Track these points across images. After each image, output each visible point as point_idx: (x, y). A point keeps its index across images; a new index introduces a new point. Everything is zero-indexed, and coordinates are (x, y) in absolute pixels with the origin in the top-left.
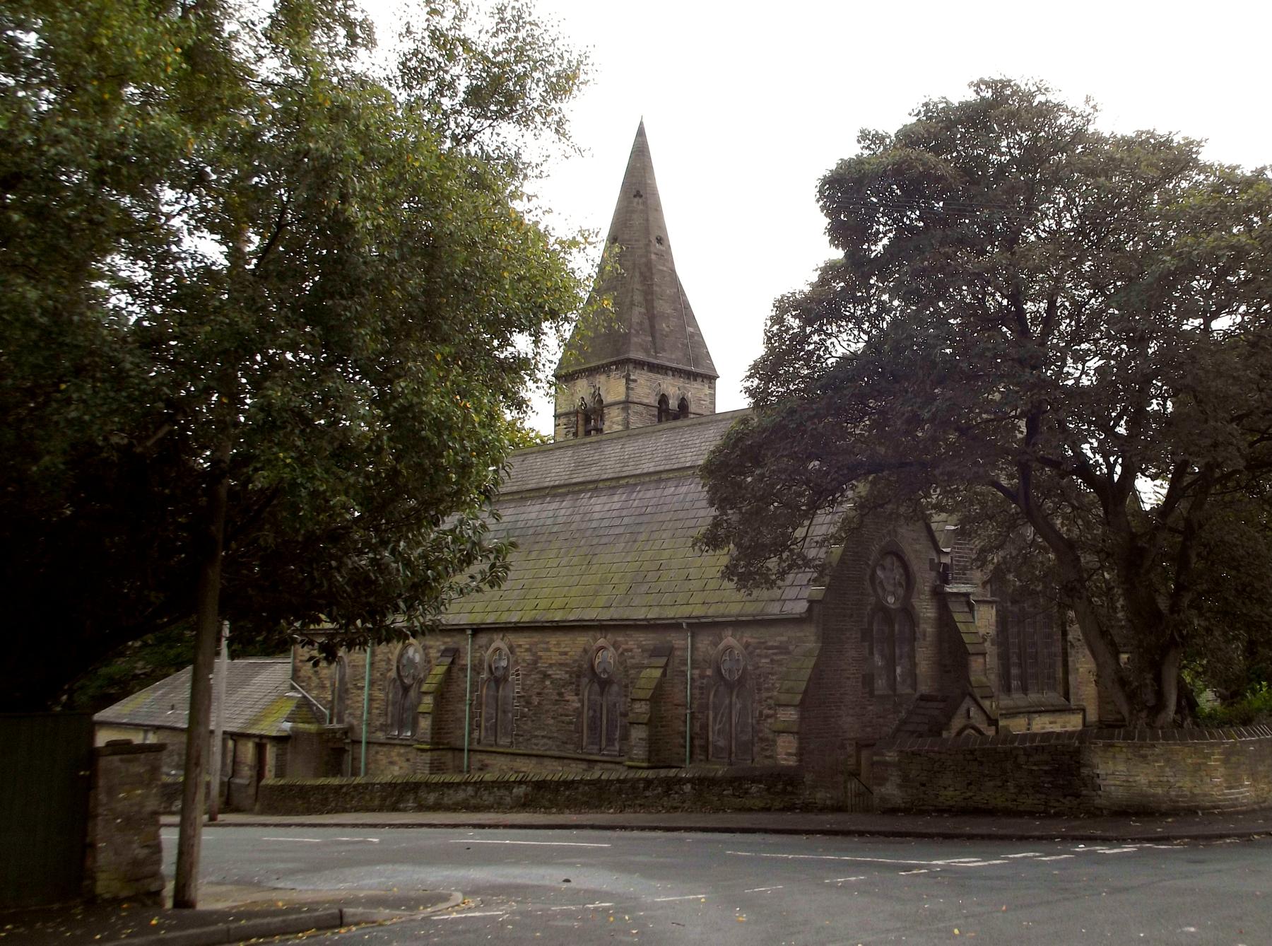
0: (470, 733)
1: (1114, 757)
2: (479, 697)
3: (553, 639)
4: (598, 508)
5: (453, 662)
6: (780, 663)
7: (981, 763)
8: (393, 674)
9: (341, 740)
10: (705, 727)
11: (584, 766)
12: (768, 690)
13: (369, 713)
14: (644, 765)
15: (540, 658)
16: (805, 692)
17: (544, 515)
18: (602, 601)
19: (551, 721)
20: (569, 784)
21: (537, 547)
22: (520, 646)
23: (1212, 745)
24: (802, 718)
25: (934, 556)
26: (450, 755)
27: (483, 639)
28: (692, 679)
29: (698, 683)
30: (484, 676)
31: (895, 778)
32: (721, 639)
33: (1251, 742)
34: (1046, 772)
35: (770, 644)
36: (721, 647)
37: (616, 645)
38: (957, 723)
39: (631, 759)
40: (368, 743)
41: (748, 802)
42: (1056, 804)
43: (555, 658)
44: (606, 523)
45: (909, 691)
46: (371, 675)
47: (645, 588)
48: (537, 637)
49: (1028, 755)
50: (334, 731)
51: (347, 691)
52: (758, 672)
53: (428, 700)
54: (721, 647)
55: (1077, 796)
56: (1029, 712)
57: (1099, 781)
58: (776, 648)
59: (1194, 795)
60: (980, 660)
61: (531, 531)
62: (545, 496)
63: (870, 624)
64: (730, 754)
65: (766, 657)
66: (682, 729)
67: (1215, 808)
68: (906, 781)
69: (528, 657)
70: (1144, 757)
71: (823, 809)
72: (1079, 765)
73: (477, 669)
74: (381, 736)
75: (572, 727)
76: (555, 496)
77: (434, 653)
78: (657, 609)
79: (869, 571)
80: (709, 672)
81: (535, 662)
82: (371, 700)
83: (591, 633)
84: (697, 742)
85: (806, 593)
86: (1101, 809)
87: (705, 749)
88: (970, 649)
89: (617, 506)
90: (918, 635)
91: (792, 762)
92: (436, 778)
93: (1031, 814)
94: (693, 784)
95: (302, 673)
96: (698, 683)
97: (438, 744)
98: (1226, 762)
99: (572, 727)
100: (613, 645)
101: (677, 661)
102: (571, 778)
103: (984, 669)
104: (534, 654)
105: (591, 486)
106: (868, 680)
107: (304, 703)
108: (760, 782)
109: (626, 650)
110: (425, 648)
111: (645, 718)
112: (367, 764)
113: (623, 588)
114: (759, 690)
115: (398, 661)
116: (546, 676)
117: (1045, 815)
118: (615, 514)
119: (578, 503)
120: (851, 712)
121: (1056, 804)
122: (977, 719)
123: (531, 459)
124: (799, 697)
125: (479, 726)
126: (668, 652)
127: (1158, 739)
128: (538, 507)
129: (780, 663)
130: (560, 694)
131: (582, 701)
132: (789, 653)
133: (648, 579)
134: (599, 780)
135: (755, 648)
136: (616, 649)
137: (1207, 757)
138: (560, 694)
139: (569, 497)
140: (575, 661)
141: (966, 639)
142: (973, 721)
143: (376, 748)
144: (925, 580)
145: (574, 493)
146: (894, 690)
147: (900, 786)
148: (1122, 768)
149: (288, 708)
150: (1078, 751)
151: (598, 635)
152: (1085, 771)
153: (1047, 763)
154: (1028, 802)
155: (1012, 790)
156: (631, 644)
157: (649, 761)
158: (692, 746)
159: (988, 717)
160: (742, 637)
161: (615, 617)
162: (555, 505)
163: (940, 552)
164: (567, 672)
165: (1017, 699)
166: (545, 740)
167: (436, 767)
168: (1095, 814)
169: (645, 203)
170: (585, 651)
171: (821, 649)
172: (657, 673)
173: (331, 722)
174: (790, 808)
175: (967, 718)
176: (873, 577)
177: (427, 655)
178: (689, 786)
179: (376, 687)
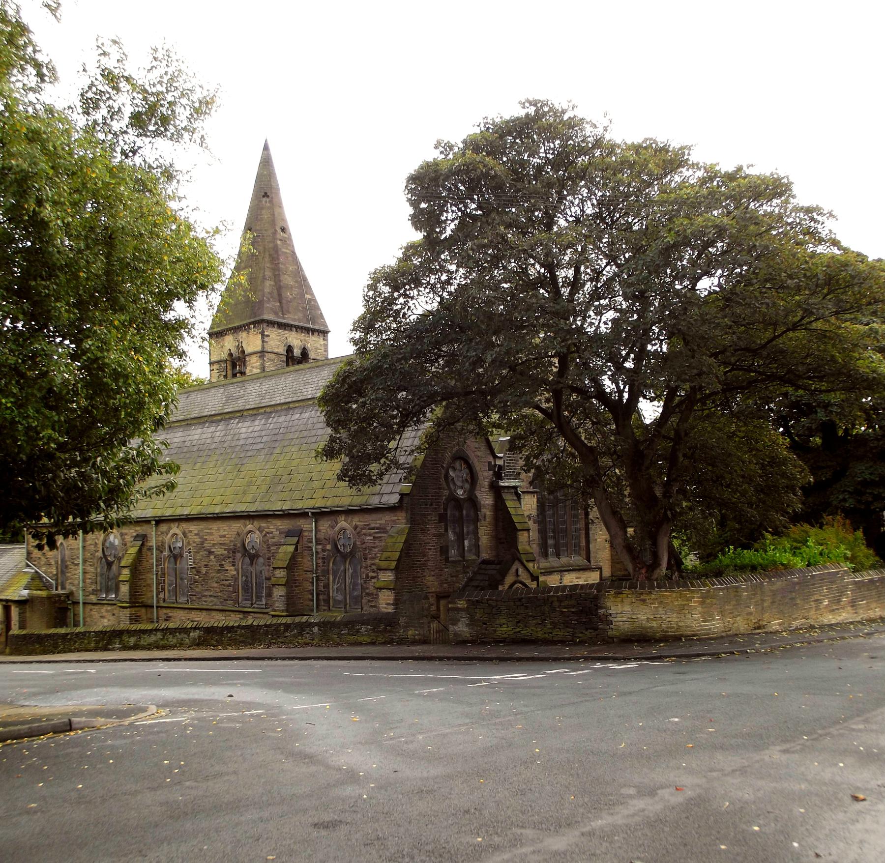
0: (157, 595)
2: (163, 569)
3: (214, 526)
5: (142, 545)
7: (527, 607)
8: (100, 554)
9: (64, 601)
10: (327, 586)
11: (241, 616)
12: (372, 559)
13: (84, 581)
15: (206, 539)
16: (399, 560)
18: (249, 498)
19: (216, 585)
22: (191, 532)
23: (693, 591)
24: (397, 578)
26: (143, 610)
27: (163, 527)
28: (316, 552)
30: (166, 553)
32: (337, 523)
34: (573, 613)
35: (373, 526)
36: (337, 529)
37: (260, 529)
39: (275, 611)
40: (84, 603)
42: (581, 635)
43: (217, 540)
46: (84, 555)
47: (280, 488)
48: (203, 525)
49: (560, 601)
50: (59, 596)
51: (67, 567)
52: (364, 546)
53: (126, 572)
54: (337, 529)
55: (596, 629)
57: (611, 619)
58: (377, 528)
64: (346, 605)
65: (370, 535)
66: (310, 588)
68: (472, 622)
69: (197, 539)
73: (160, 549)
74: (93, 598)
75: (231, 589)
77: (128, 538)
78: (289, 502)
80: (329, 547)
81: (202, 543)
82: (85, 573)
83: (242, 521)
84: (321, 597)
85: (398, 489)
86: (613, 638)
87: (327, 601)
91: (390, 609)
92: (134, 627)
93: (563, 642)
95: (34, 555)
96: (321, 556)
97: (134, 603)
99: (231, 589)
100: (259, 530)
101: (305, 539)
107: (37, 577)
109: (268, 533)
110: (122, 535)
111: (284, 581)
112: (84, 618)
113: (264, 488)
114: (366, 559)
115: (103, 544)
121: (581, 635)
124: (394, 564)
125: (163, 589)
126: (299, 533)
130: (221, 565)
132: (386, 532)
135: (362, 529)
136: (261, 532)
137: (689, 600)
138: (221, 565)
140: (231, 541)
143: (90, 607)
147: (467, 625)
148: (627, 608)
149: (25, 580)
150: (596, 598)
151: (247, 522)
152: (601, 611)
154: (560, 634)
155: (549, 626)
156: (272, 528)
157: (287, 611)
158: (318, 600)
160: (352, 521)
161: (259, 509)
164: (225, 550)
166: (212, 599)
167: (134, 619)
168: (609, 641)
170: (238, 534)
172: (291, 549)
173: (57, 589)
177: (123, 540)
179: (88, 564)
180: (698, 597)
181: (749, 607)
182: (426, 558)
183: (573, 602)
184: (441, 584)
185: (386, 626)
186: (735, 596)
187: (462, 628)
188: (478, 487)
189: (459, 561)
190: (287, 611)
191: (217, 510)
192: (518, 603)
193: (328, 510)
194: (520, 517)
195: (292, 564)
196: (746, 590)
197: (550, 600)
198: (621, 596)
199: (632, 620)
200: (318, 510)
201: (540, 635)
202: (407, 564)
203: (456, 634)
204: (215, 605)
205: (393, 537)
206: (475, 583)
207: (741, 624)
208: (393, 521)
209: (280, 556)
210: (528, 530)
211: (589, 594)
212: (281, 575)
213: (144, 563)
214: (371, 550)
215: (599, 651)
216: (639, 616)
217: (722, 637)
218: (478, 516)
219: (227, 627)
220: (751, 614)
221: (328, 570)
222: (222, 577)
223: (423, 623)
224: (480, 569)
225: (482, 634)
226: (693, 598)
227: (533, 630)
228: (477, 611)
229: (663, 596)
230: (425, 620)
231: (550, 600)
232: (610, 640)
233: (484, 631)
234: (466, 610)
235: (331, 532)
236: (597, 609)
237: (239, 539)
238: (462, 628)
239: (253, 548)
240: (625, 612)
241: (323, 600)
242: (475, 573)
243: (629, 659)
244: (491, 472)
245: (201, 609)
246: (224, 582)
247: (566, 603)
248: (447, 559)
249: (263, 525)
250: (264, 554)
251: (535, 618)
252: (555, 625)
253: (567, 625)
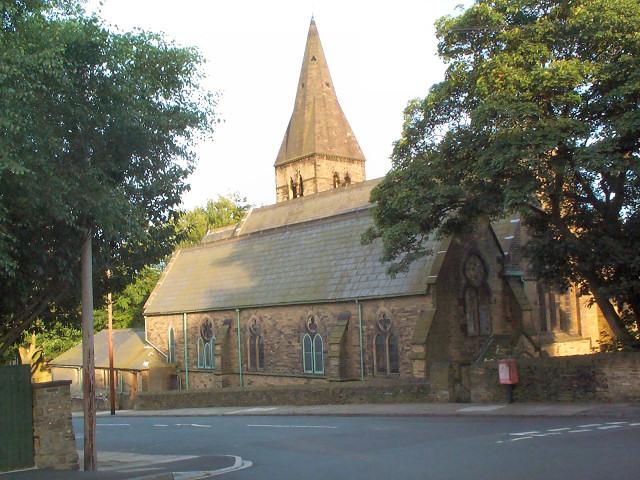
3: (283, 312)
12: (406, 336)
15: (277, 323)
19: (285, 357)
24: (427, 350)
27: (245, 314)
29: (365, 334)
35: (406, 309)
43: (285, 322)
48: (274, 312)
54: (378, 313)
58: (410, 312)
60: (529, 313)
66: (358, 359)
69: (270, 323)
80: (372, 327)
81: (275, 325)
83: (304, 308)
84: (367, 366)
88: (524, 308)
91: (422, 375)
96: (365, 334)
101: (353, 322)
106: (464, 328)
114: (401, 336)
116: (281, 333)
138: (290, 342)
144: (494, 267)
151: (308, 308)
156: (327, 313)
157: (341, 377)
170: (302, 318)
210: (530, 310)
213: (232, 341)
249: (320, 310)
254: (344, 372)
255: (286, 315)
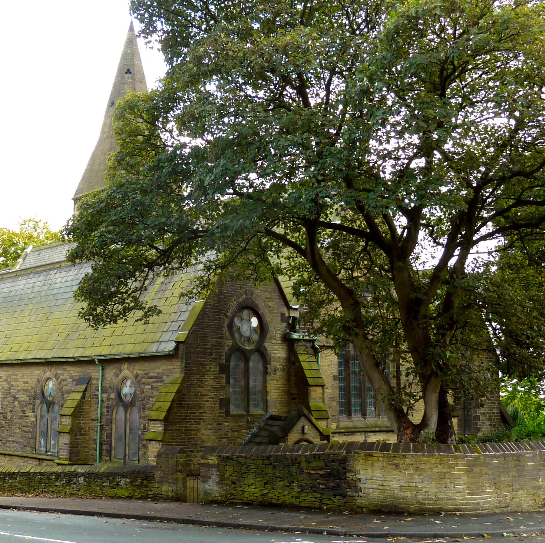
1: (373, 465)
3: (20, 372)
4: (59, 280)
6: (157, 389)
7: (275, 467)
10: (109, 436)
11: (36, 462)
12: (149, 409)
14: (67, 462)
15: (12, 386)
16: (169, 411)
17: (27, 286)
18: (49, 345)
19: (18, 431)
20: (12, 475)
21: (19, 309)
23: (456, 457)
24: (166, 430)
25: (285, 310)
28: (102, 401)
29: (105, 404)
31: (215, 477)
32: (121, 371)
33: (495, 457)
34: (321, 476)
35: (151, 375)
36: (120, 377)
37: (57, 376)
38: (293, 437)
39: (60, 459)
41: (119, 493)
42: (328, 502)
43: (21, 385)
44: (62, 290)
45: (261, 412)
48: (10, 371)
49: (308, 462)
52: (143, 395)
54: (120, 377)
55: (344, 496)
56: (366, 432)
57: (360, 485)
59: (438, 499)
60: (319, 390)
61: (18, 297)
62: (30, 274)
63: (228, 360)
64: (125, 456)
65: (148, 384)
67: (457, 510)
68: (222, 481)
70: (397, 465)
71: (167, 499)
72: (346, 470)
75: (30, 435)
76: (36, 273)
78: (81, 349)
79: (227, 321)
80: (113, 396)
81: (10, 389)
83: (42, 368)
84: (104, 447)
85: (174, 338)
86: (361, 508)
87: (109, 452)
89: (70, 278)
90: (269, 370)
91: (154, 464)
93: (308, 509)
94: (85, 477)
96: (105, 404)
98: (469, 472)
99: (30, 435)
100: (55, 377)
101: (93, 387)
102: (12, 471)
103: (325, 395)
104: (9, 383)
105: (57, 266)
106: (224, 403)
108: (127, 478)
109: (63, 380)
111: (68, 429)
114: (144, 409)
116: (16, 399)
117: (320, 510)
118: (68, 284)
119: (48, 278)
120: (209, 426)
121: (328, 502)
122: (311, 434)
123: (43, 253)
124: (163, 415)
126: (88, 381)
127: (409, 451)
128: (24, 282)
129: (157, 389)
130: (24, 412)
131: (36, 416)
132: (162, 381)
133: (79, 329)
134: (28, 473)
135: (142, 378)
136: (57, 379)
137: (452, 467)
138: (24, 412)
139: (43, 274)
140: (32, 388)
141: (308, 374)
142: (307, 437)
144: (277, 328)
145: (47, 270)
146: (248, 411)
147: (218, 483)
148: (378, 474)
150: (345, 460)
151: (46, 369)
152: (350, 476)
153: (321, 469)
154: (308, 499)
155: (296, 489)
156: (66, 376)
157: (70, 459)
158: (101, 449)
159: (321, 434)
161: (56, 356)
162: (34, 280)
163: (289, 308)
165: (357, 420)
166: (14, 444)
168: (357, 511)
169: (133, 78)
170: (38, 380)
171: (184, 378)
172: (79, 396)
174: (144, 498)
175: (303, 431)
176: (231, 326)
178: (82, 478)
180: (463, 465)
181: (537, 480)
182: (202, 410)
183: (321, 464)
184: (220, 438)
185: (143, 480)
186: (516, 465)
187: (212, 486)
188: (267, 340)
189: (244, 415)
190: (70, 459)
191: (21, 356)
192: (266, 462)
193: (112, 357)
194: (314, 372)
195: (78, 412)
196: (532, 459)
197: (299, 460)
198: (371, 458)
199: (383, 488)
200: (103, 358)
201: (287, 499)
202: (179, 414)
203: (206, 493)
204: (16, 451)
205: (167, 387)
206: (258, 440)
207: (524, 500)
208: (170, 370)
209: (68, 403)
211: (338, 455)
212: (67, 423)
214: (149, 399)
215: (331, 522)
216: (391, 483)
217: (495, 514)
218: (267, 368)
219: (9, 473)
220: (539, 488)
221: (111, 419)
222: (24, 423)
223: (177, 479)
224: (266, 424)
225: (232, 494)
226: (457, 465)
227: (279, 493)
228: (227, 468)
229: (420, 461)
230: (180, 476)
231: (299, 460)
232: (359, 510)
233: (232, 492)
234: (217, 466)
235: (115, 381)
236: (345, 473)
237: (39, 386)
238: (212, 486)
239: (50, 395)
240: (375, 480)
241: (106, 449)
242: (260, 429)
243: (351, 535)
244: (285, 324)
245: (5, 455)
246: (25, 428)
247: (314, 464)
248: (227, 413)
250: (59, 401)
251: (282, 479)
252: (302, 489)
253: (315, 489)
254: (76, 455)
255: (23, 376)
